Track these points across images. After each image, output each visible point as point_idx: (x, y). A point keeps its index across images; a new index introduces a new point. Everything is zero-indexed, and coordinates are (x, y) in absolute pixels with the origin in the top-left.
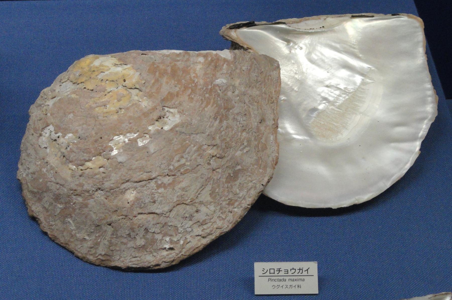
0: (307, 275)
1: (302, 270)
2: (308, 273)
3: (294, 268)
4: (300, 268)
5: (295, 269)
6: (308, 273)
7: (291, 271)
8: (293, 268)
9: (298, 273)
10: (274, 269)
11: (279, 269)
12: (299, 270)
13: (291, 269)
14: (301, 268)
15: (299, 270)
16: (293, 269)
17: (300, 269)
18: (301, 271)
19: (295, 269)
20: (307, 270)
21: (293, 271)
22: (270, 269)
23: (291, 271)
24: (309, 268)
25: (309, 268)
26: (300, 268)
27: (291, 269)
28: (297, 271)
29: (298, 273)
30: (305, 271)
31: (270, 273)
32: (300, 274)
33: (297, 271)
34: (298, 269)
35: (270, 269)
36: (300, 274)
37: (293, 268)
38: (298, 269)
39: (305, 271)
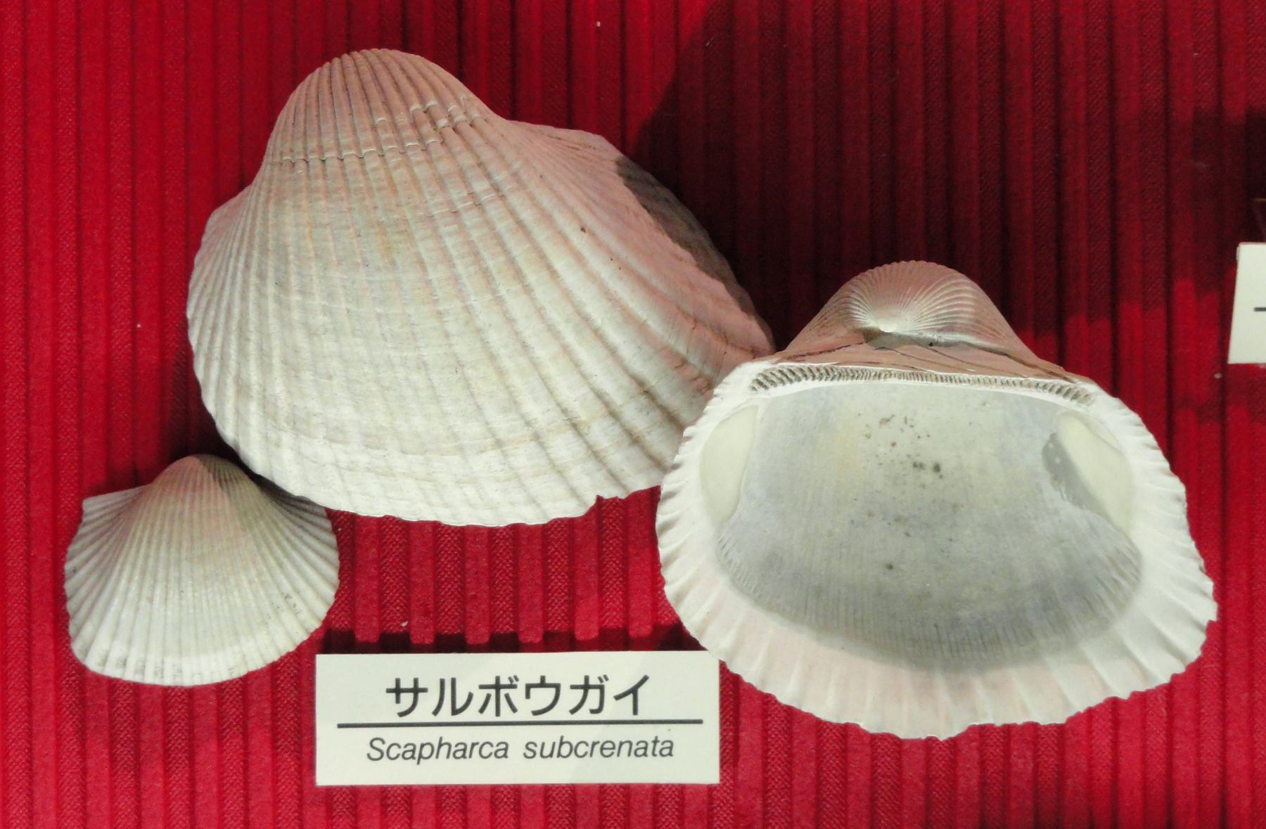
0: (629, 716)
1: (601, 688)
2: (635, 711)
3: (548, 681)
4: (587, 679)
5: (557, 687)
6: (635, 711)
7: (528, 696)
8: (543, 678)
9: (573, 711)
12: (581, 692)
13: (529, 687)
14: (594, 681)
15: (580, 692)
16: (543, 684)
17: (586, 687)
18: (594, 695)
19: (557, 687)
20: (634, 691)
21: (545, 696)
23: (528, 696)
24: (645, 679)
25: (645, 679)
26: (587, 679)
27: (529, 687)
28: (570, 698)
29: (573, 711)
30: (618, 697)
32: (584, 714)
33: (570, 698)
34: (573, 687)
36: (584, 714)
37: (543, 678)
38: (573, 687)
39: (618, 697)
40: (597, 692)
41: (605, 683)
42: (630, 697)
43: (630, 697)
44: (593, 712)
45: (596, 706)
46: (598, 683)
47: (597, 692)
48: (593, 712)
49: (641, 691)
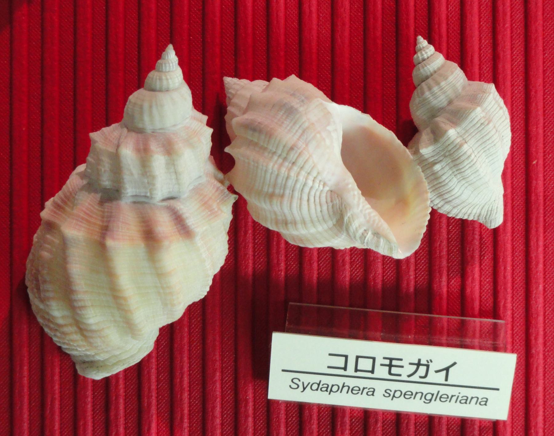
0: (444, 382)
1: (428, 366)
2: (446, 379)
4: (419, 360)
6: (446, 379)
10: (374, 359)
11: (391, 360)
12: (415, 367)
14: (423, 362)
15: (415, 367)
17: (419, 364)
18: (422, 370)
20: (447, 369)
22: (358, 357)
24: (455, 364)
25: (455, 364)
26: (419, 360)
30: (437, 372)
31: (356, 370)
35: (358, 357)
36: (415, 378)
39: (437, 372)
40: (425, 368)
41: (430, 363)
42: (445, 372)
43: (445, 372)
44: (421, 377)
45: (423, 375)
46: (426, 363)
47: (425, 368)
48: (421, 377)
49: (451, 370)
